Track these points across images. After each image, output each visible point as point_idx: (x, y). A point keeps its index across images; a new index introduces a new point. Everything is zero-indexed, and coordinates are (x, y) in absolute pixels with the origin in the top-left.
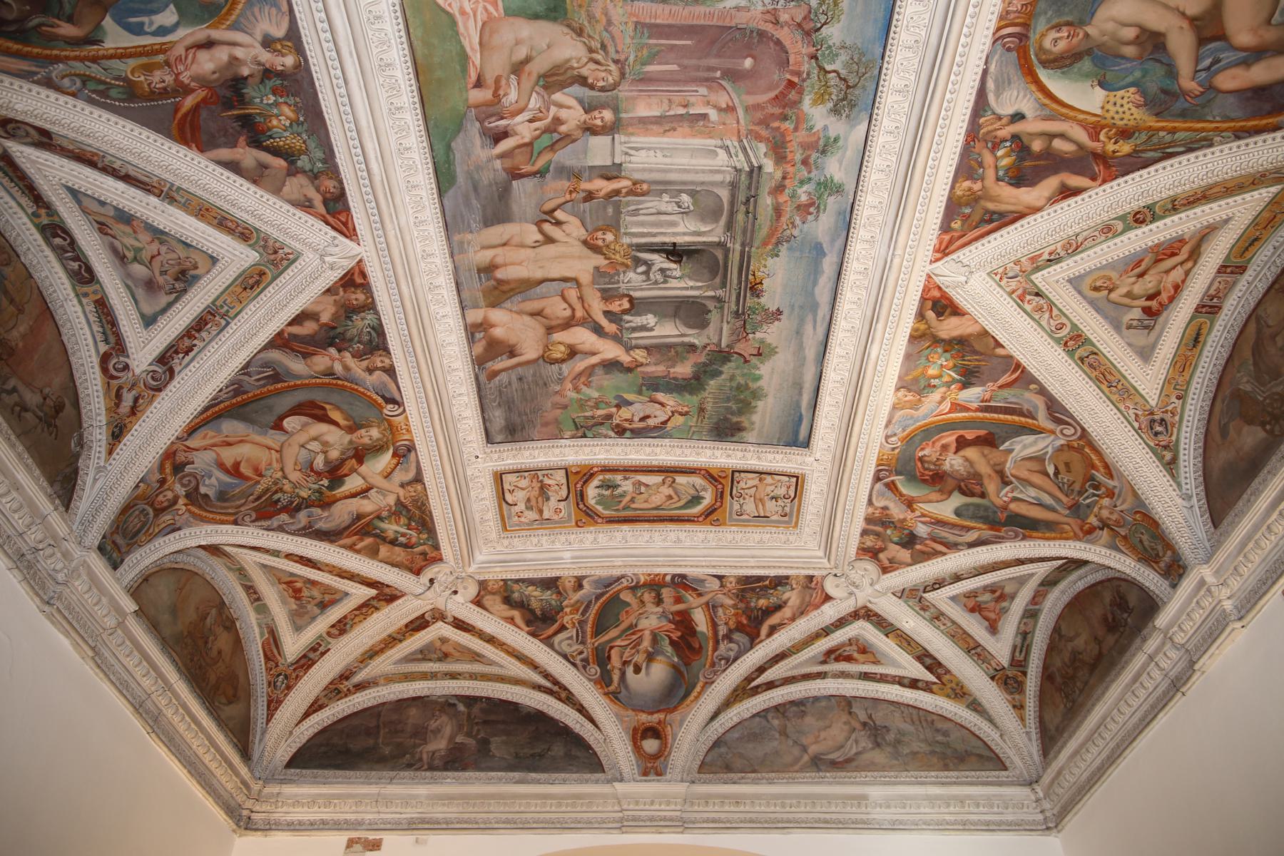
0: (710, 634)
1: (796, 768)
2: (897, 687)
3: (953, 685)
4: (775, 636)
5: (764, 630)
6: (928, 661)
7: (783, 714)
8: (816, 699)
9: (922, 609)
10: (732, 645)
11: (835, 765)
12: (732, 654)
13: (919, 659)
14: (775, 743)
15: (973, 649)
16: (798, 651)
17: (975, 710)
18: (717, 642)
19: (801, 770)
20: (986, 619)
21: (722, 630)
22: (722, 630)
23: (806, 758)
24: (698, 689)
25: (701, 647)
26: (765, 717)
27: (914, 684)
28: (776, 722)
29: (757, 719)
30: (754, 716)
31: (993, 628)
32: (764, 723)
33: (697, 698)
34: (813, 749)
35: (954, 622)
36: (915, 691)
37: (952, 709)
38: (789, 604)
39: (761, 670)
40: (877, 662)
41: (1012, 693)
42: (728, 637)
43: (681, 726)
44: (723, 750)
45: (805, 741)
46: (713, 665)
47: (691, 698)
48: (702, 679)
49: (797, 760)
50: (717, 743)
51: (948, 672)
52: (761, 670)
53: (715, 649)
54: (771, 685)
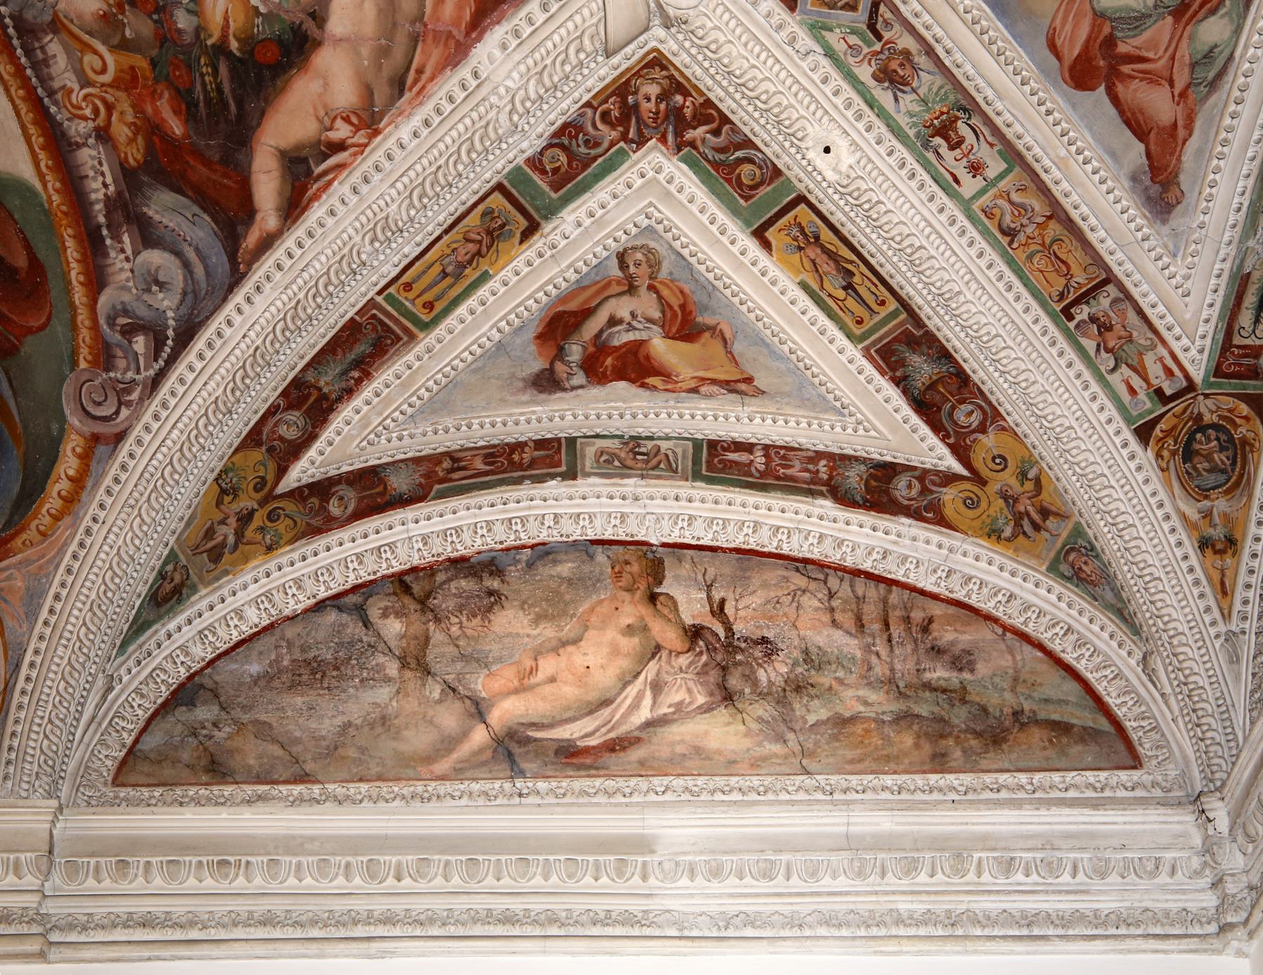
0: (52, 194)
1: (442, 766)
2: (826, 506)
3: (1008, 478)
4: (317, 212)
5: (267, 188)
6: (922, 368)
7: (422, 602)
8: (543, 552)
9: (886, 76)
10: (155, 258)
11: (571, 757)
12: (167, 304)
13: (889, 359)
14: (383, 694)
15: (1086, 301)
16: (436, 312)
17: (1078, 578)
18: (93, 245)
19: (458, 774)
20: (1137, 124)
21: (100, 185)
22: (100, 185)
23: (479, 736)
24: (68, 464)
25: (36, 266)
26: (360, 612)
27: (878, 488)
28: (393, 628)
29: (332, 617)
30: (319, 606)
31: (1161, 187)
32: (354, 628)
33: (71, 501)
34: (506, 711)
35: (1013, 156)
36: (884, 521)
37: (1003, 581)
38: (337, 24)
39: (310, 401)
40: (739, 385)
41: (1203, 493)
42: (126, 210)
43: (32, 615)
44: (204, 713)
45: (480, 684)
46: (104, 357)
47: (52, 501)
48: (74, 420)
49: (449, 743)
50: (186, 693)
51: (992, 416)
52: (310, 401)
53: (97, 281)
54: (372, 492)
